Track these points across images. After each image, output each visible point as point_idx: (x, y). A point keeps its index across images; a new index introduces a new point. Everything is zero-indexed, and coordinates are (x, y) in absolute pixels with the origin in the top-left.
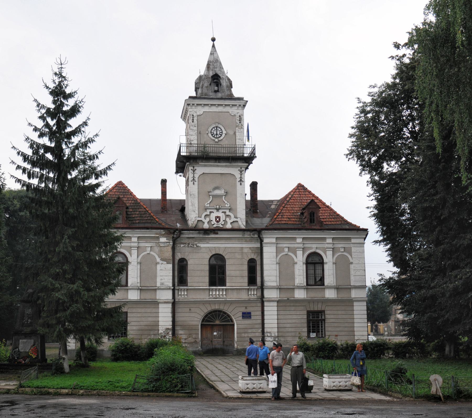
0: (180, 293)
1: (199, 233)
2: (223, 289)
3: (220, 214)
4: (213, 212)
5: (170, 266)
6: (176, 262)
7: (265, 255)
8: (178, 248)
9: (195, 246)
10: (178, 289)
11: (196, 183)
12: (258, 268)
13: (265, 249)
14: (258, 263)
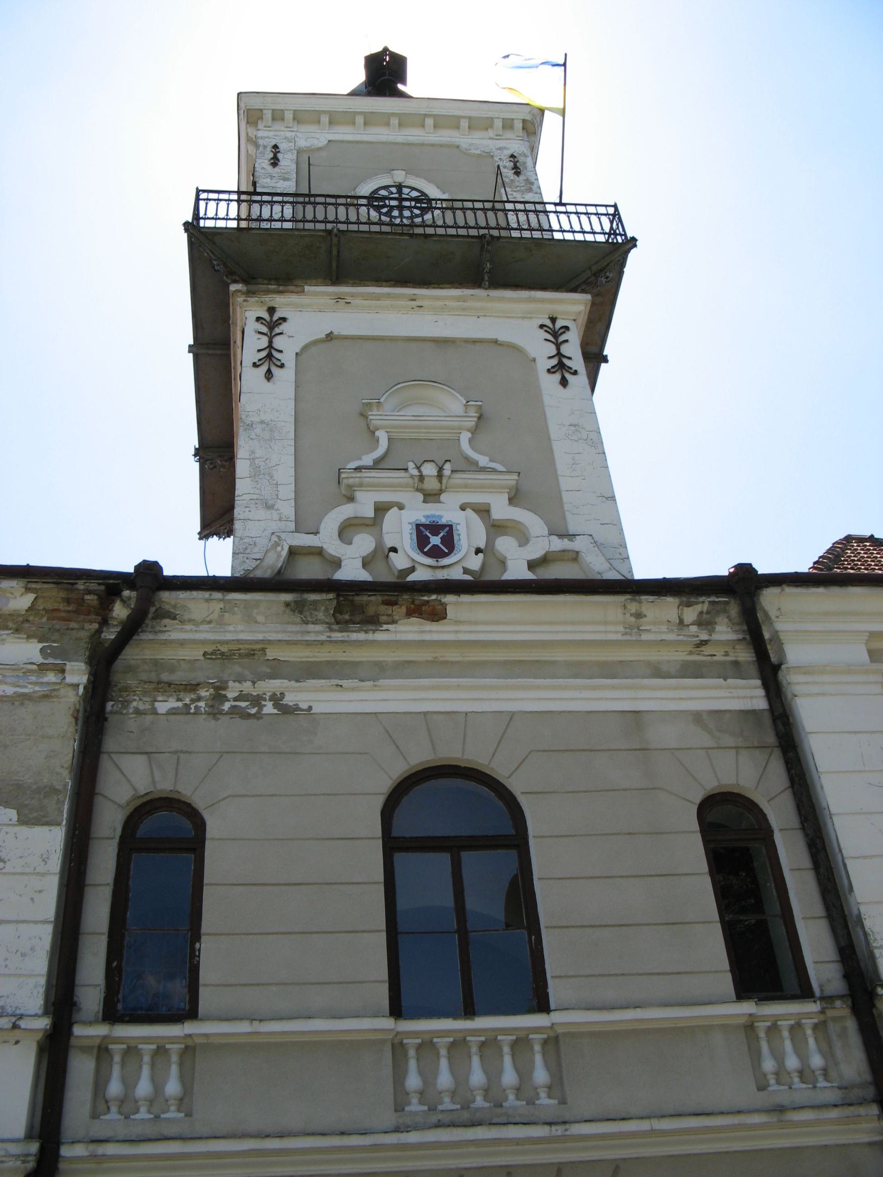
0: (115, 1088)
1: (298, 608)
2: (521, 1043)
3: (447, 511)
4: (401, 507)
5: (51, 841)
6: (109, 821)
7: (824, 752)
8: (132, 723)
9: (269, 708)
10: (102, 1051)
11: (286, 377)
12: (790, 852)
13: (812, 713)
14: (780, 814)
